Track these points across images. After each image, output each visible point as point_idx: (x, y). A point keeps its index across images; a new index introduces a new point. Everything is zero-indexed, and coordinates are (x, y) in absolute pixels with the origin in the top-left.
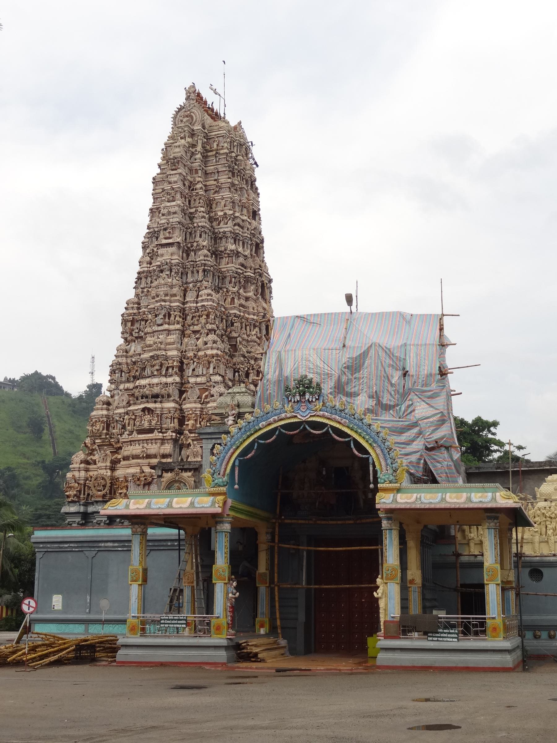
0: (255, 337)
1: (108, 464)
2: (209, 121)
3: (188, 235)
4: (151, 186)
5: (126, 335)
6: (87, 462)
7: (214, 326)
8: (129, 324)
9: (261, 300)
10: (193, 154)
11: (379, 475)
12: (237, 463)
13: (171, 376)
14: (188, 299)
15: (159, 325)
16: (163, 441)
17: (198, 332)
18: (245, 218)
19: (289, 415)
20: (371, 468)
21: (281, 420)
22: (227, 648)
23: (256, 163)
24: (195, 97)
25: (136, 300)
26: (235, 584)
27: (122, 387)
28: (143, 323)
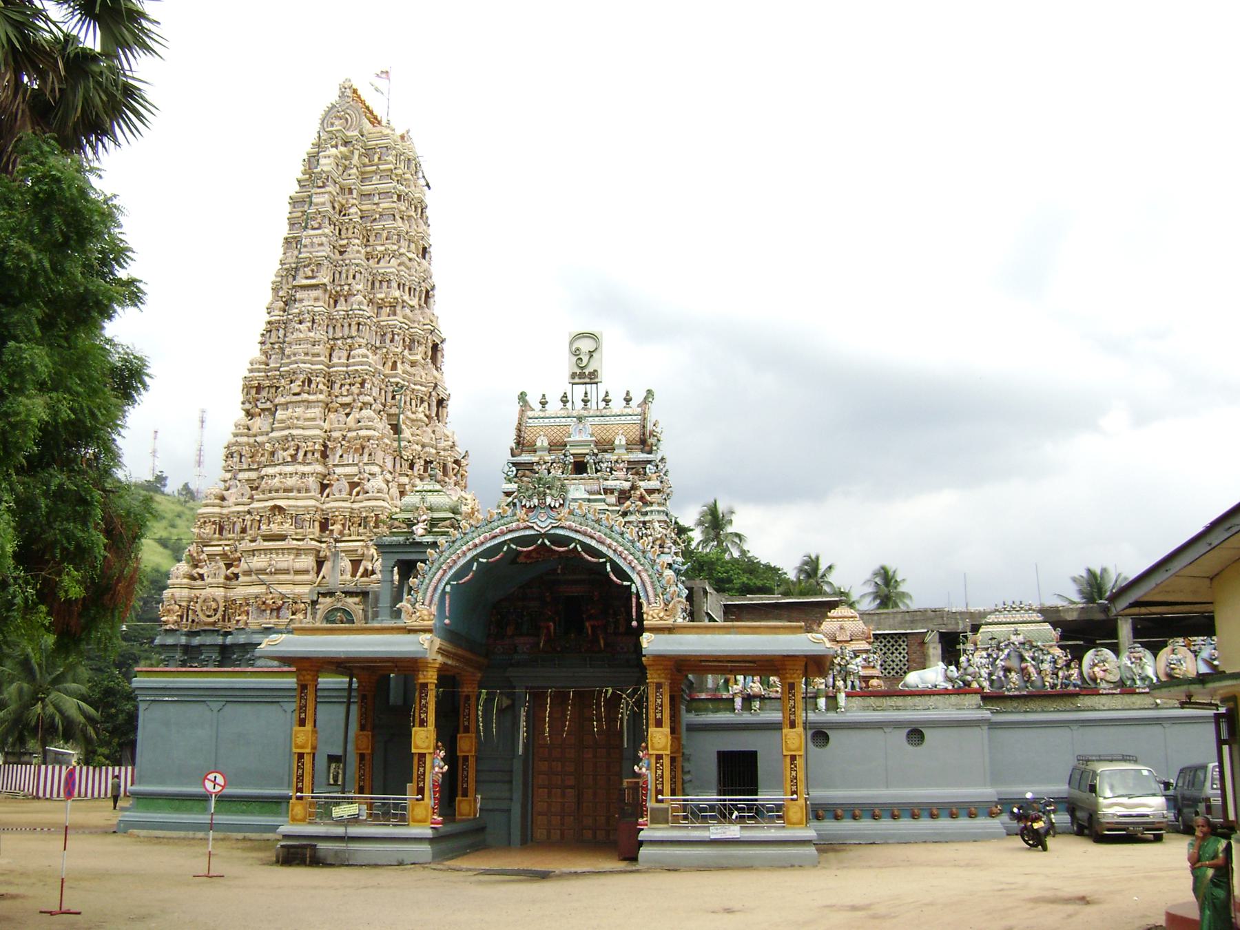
0: (422, 416)
1: (222, 580)
2: (367, 126)
3: (337, 275)
4: (288, 208)
5: (248, 406)
6: (193, 578)
7: (371, 399)
8: (254, 391)
9: (431, 366)
10: (346, 168)
11: (645, 609)
12: (448, 588)
13: (309, 464)
14: (335, 360)
15: (295, 394)
16: (298, 552)
17: (348, 405)
18: (411, 255)
19: (522, 525)
20: (634, 600)
21: (511, 531)
22: (431, 841)
23: (428, 185)
24: (351, 95)
25: (264, 358)
26: (442, 754)
27: (241, 476)
28: (273, 390)
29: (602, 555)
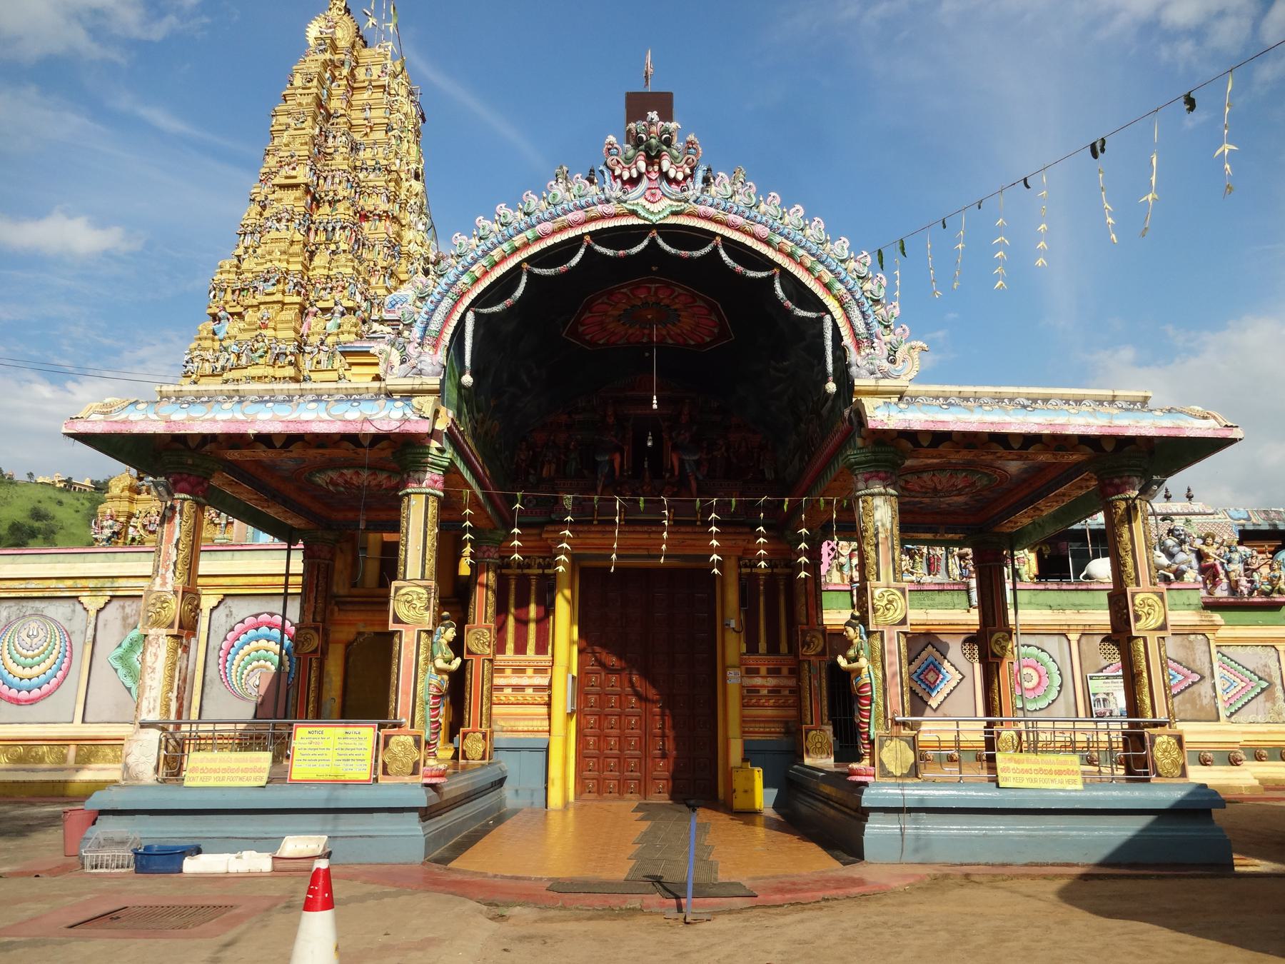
11: (853, 356)
29: (768, 264)
